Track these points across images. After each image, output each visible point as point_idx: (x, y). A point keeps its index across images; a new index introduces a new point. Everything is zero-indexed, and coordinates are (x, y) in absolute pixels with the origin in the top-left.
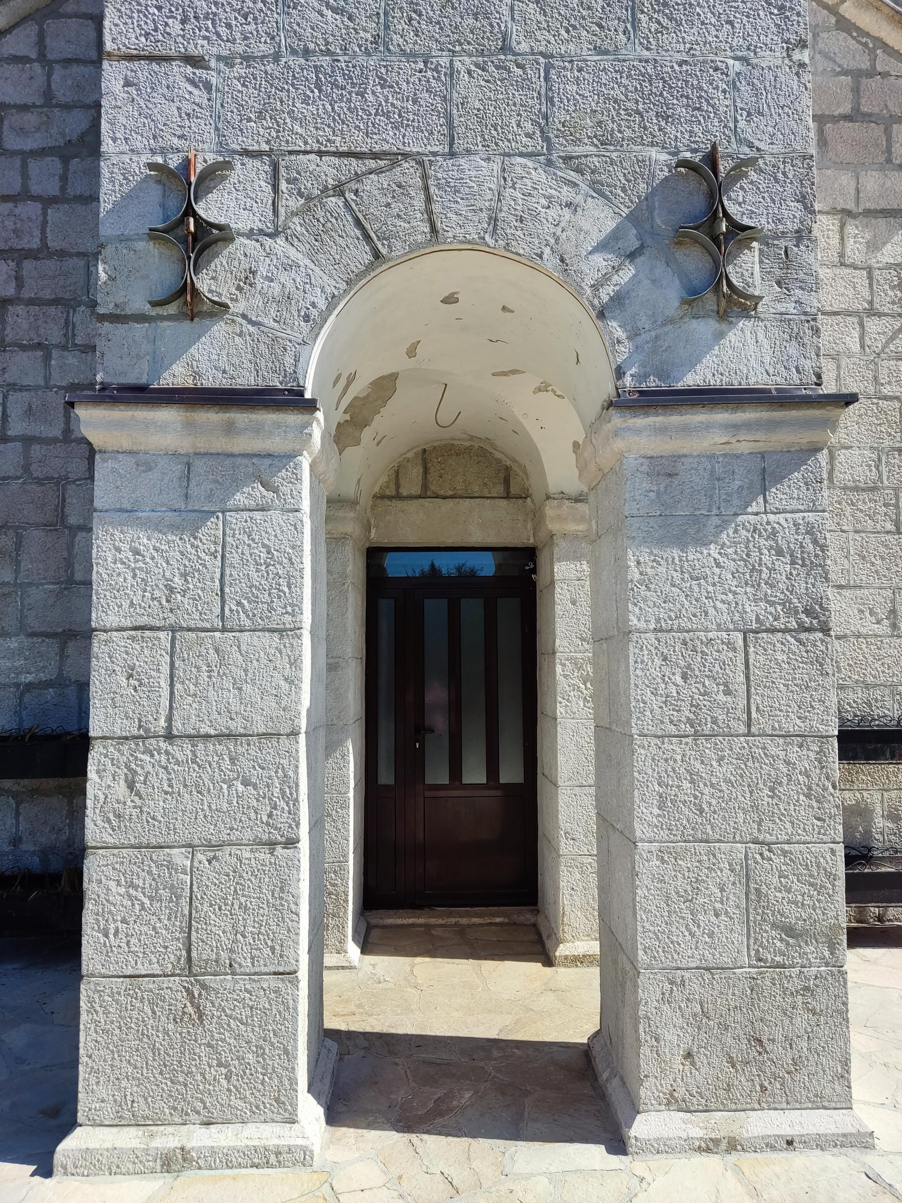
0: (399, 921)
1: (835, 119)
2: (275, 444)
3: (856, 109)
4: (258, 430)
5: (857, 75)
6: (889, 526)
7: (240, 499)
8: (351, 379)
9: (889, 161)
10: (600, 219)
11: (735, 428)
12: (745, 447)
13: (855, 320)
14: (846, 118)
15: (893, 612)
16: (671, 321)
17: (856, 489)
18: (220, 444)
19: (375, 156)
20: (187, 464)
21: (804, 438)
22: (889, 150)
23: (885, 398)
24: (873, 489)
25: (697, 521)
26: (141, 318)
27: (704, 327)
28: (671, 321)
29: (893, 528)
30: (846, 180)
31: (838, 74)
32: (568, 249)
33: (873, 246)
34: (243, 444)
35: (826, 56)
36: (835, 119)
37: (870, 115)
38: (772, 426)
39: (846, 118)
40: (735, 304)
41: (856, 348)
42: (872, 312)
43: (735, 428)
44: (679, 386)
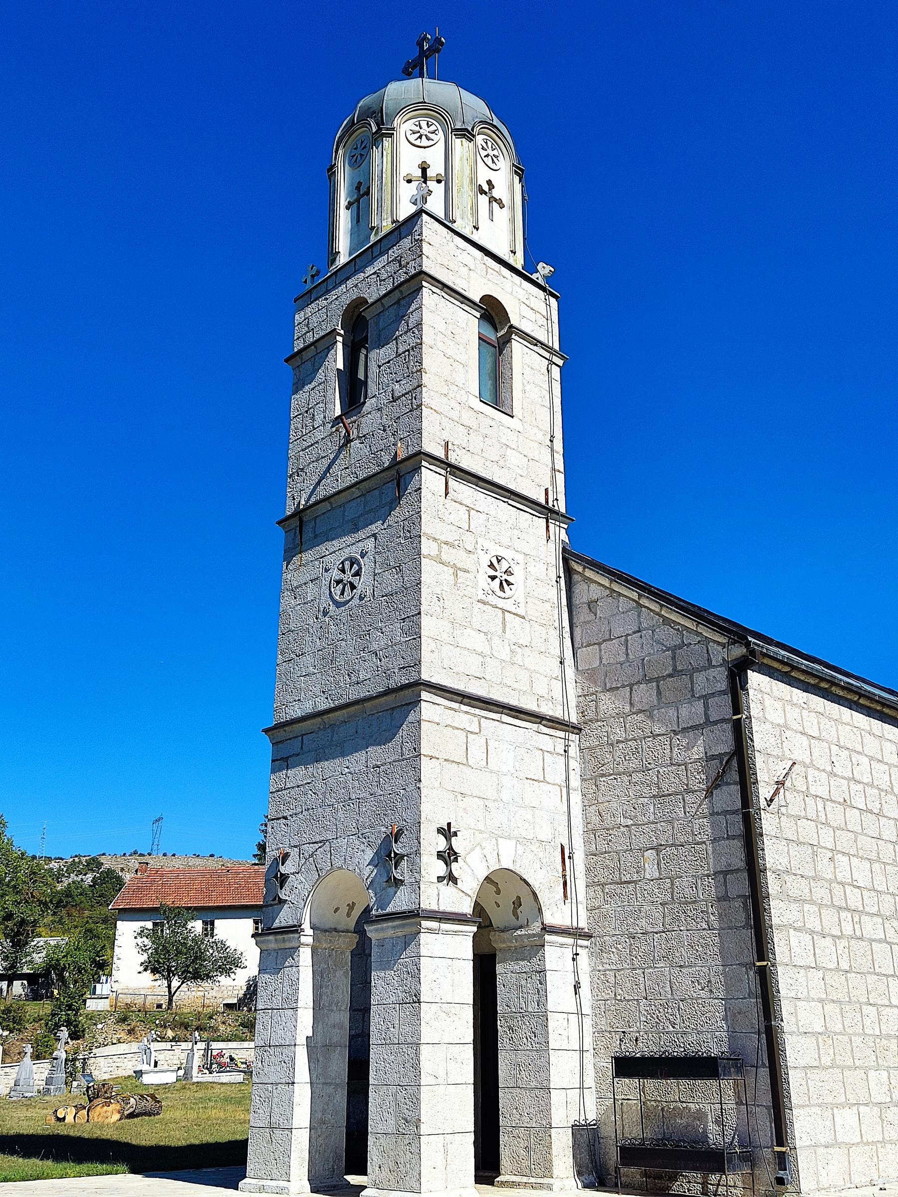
0: (486, 1174)
1: (664, 678)
2: (294, 944)
3: (675, 669)
4: (289, 940)
5: (674, 649)
6: (705, 926)
7: (287, 964)
8: (351, 907)
9: (693, 696)
10: (369, 854)
11: (394, 927)
12: (400, 934)
13: (680, 797)
14: (670, 676)
15: (709, 982)
16: (384, 889)
17: (686, 903)
18: (282, 946)
19: (320, 842)
20: (276, 951)
21: (414, 929)
22: (692, 690)
23: (698, 844)
24: (694, 902)
25: (388, 962)
26: (271, 905)
27: (391, 890)
28: (384, 889)
29: (706, 927)
30: (672, 712)
31: (664, 651)
32: (361, 866)
33: (688, 748)
34: (288, 945)
35: (658, 642)
36: (664, 678)
37: (682, 671)
38: (403, 926)
39: (670, 676)
40: (398, 883)
41: (682, 815)
42: (689, 791)
43: (394, 927)
44: (388, 910)
